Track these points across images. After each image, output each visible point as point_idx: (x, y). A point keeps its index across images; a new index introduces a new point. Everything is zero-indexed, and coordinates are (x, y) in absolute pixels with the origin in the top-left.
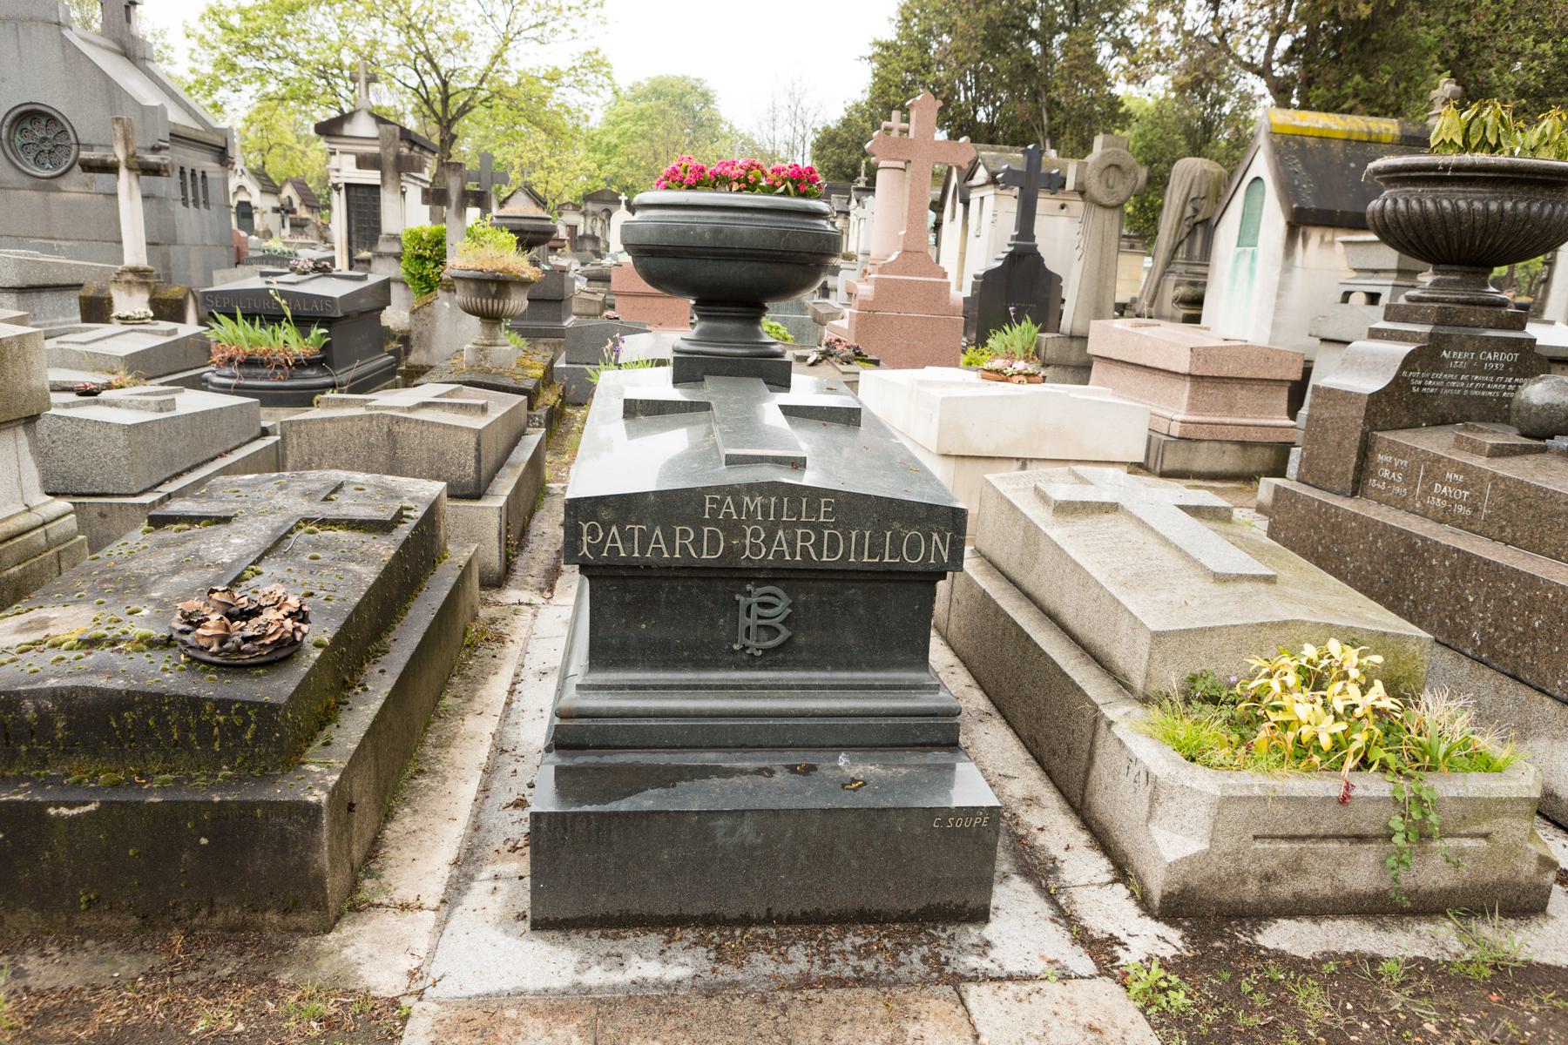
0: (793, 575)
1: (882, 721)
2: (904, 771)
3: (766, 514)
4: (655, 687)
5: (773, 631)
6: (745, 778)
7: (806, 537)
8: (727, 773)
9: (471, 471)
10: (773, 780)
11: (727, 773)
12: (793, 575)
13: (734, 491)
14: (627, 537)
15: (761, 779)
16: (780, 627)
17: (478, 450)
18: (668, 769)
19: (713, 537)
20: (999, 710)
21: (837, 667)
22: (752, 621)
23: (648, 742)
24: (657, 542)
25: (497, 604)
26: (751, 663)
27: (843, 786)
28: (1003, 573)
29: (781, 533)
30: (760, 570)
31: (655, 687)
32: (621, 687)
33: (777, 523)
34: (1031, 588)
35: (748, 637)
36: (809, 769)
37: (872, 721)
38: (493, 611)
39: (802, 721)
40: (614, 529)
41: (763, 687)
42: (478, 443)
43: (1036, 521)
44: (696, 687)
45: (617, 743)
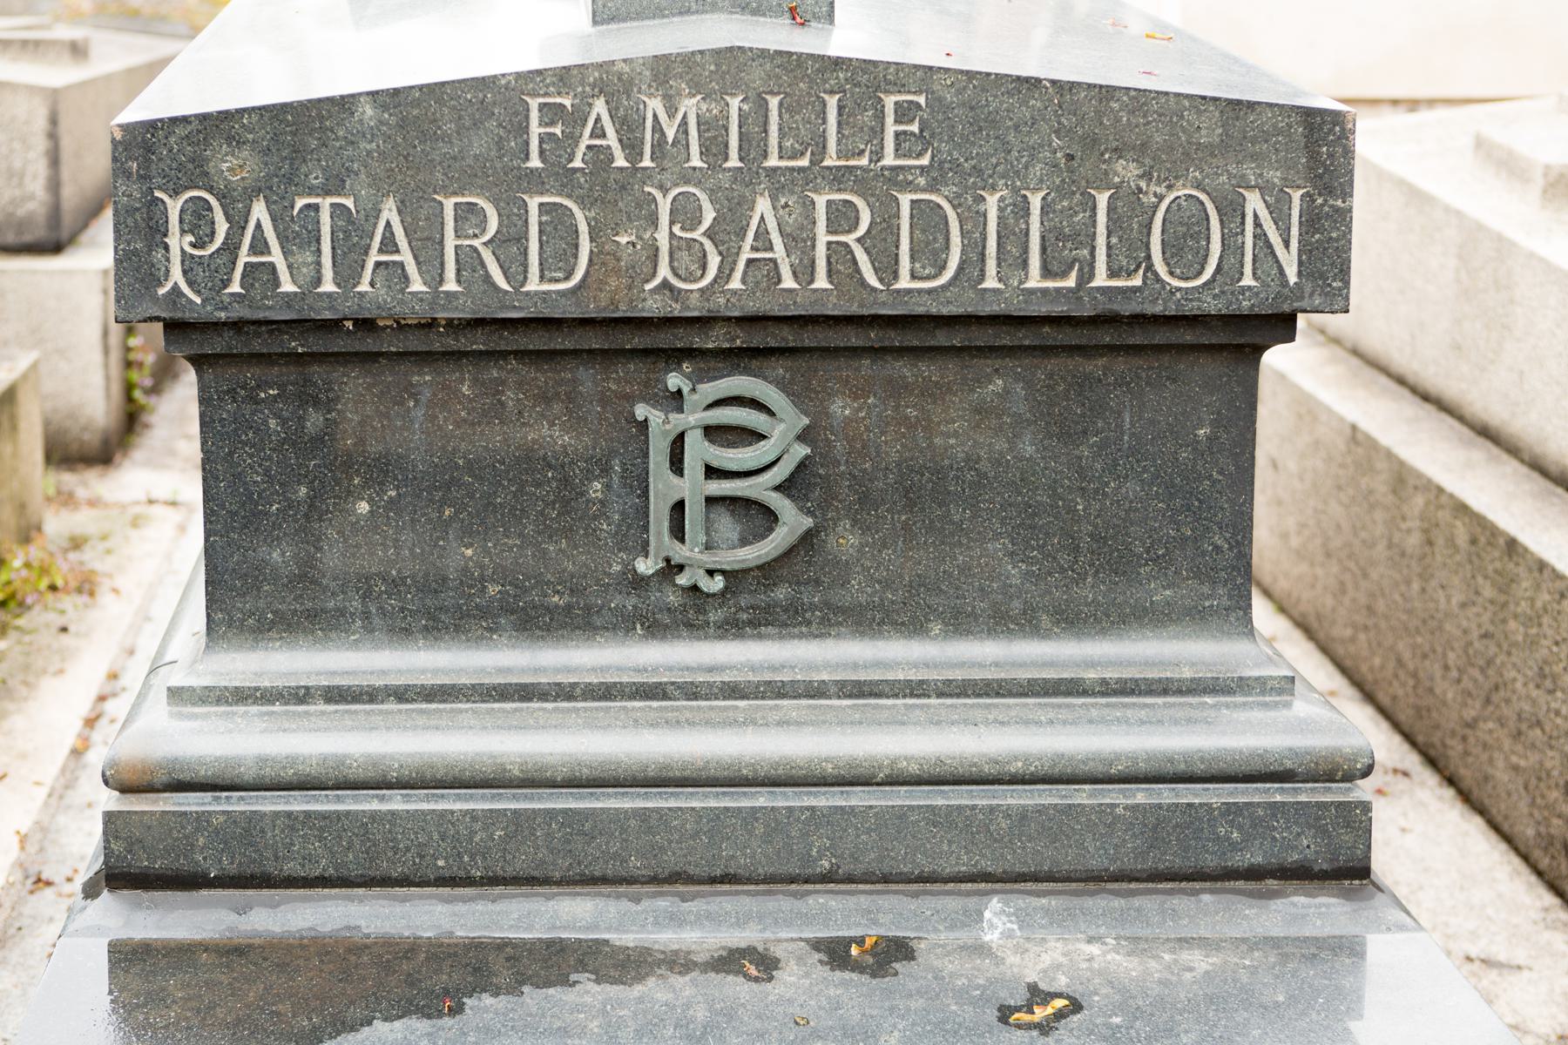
0: (809, 338)
1: (1114, 796)
2: (1200, 961)
3: (714, 149)
4: (401, 694)
5: (757, 516)
6: (684, 986)
7: (842, 217)
8: (627, 966)
9: (36, 185)
10: (774, 990)
11: (627, 966)
12: (809, 338)
13: (611, 82)
14: (298, 235)
15: (735, 987)
16: (778, 502)
17: (53, 136)
18: (443, 953)
19: (557, 224)
20: (1432, 762)
21: (960, 623)
22: (692, 487)
23: (384, 867)
24: (389, 245)
25: (93, 503)
26: (693, 614)
27: (1005, 1013)
28: (1401, 381)
29: (763, 206)
30: (703, 322)
31: (401, 694)
32: (301, 696)
33: (752, 174)
34: (1494, 411)
35: (678, 532)
36: (891, 953)
37: (1083, 796)
38: (80, 521)
39: (858, 798)
40: (259, 211)
41: (733, 691)
42: (54, 121)
43: (1496, 223)
44: (526, 693)
45: (291, 868)
